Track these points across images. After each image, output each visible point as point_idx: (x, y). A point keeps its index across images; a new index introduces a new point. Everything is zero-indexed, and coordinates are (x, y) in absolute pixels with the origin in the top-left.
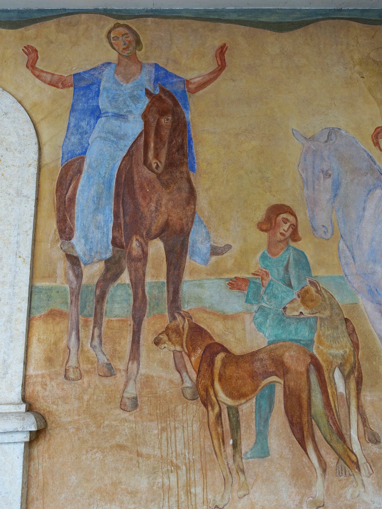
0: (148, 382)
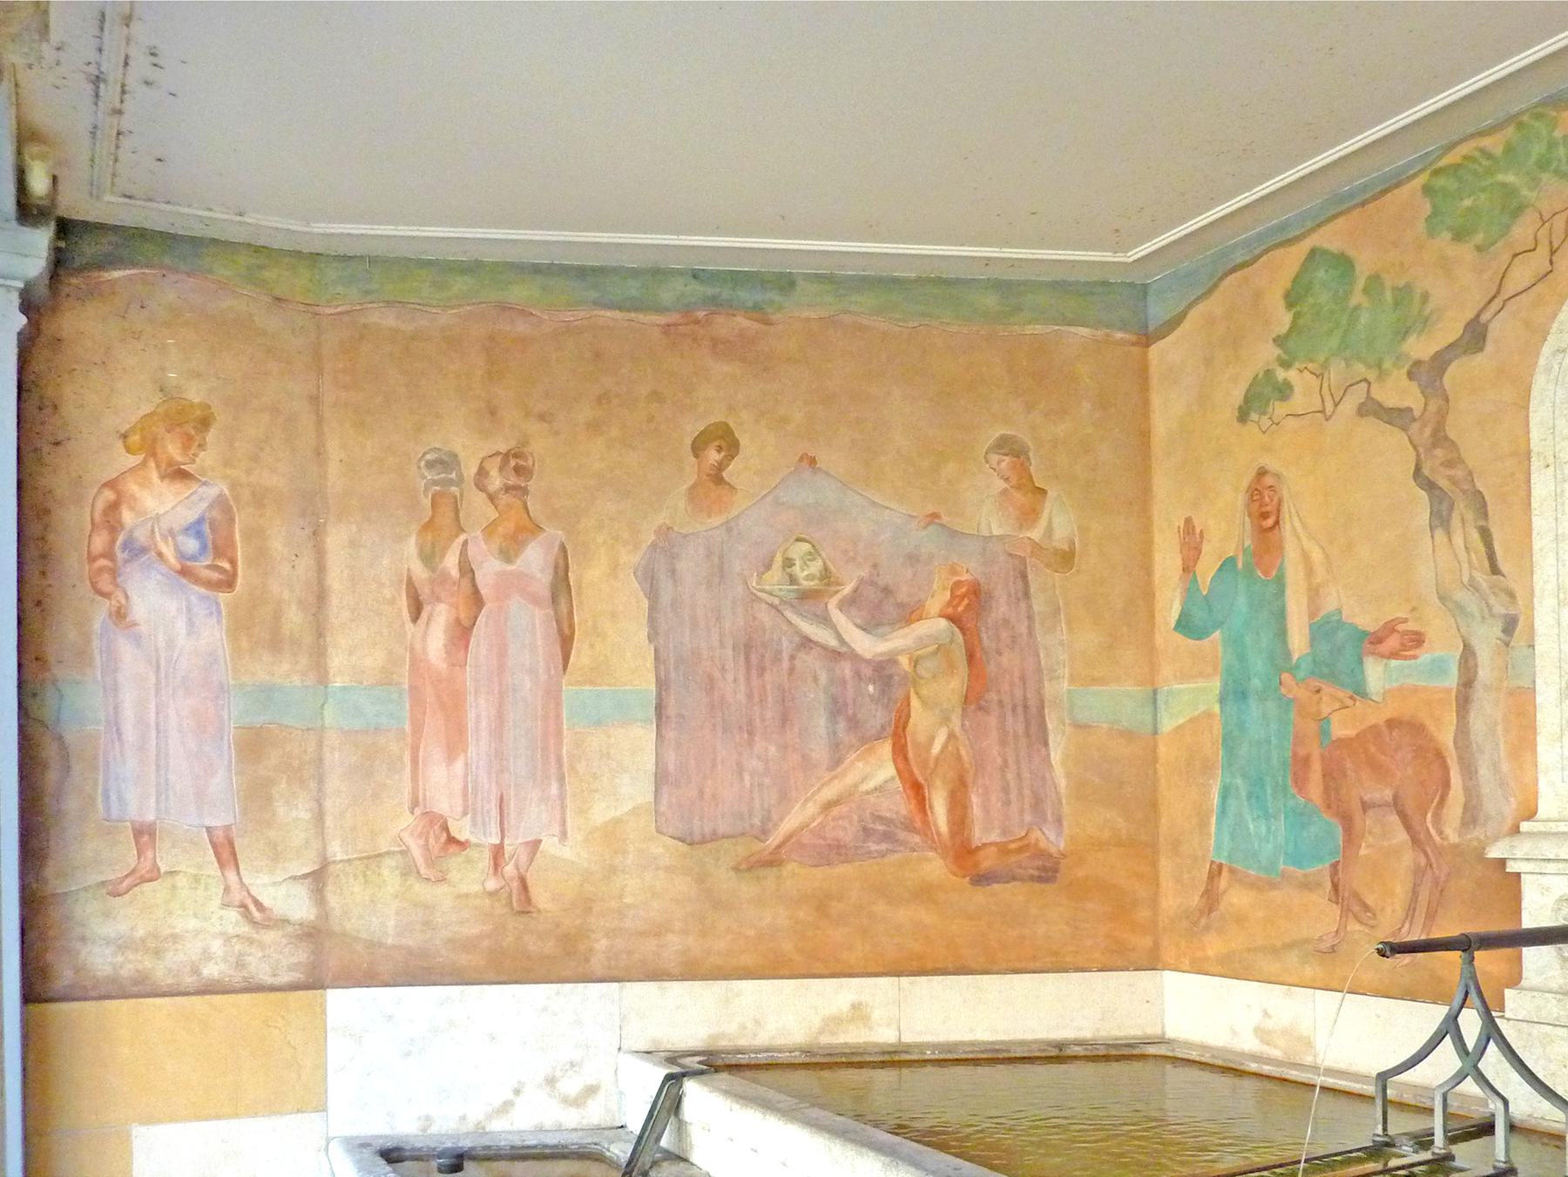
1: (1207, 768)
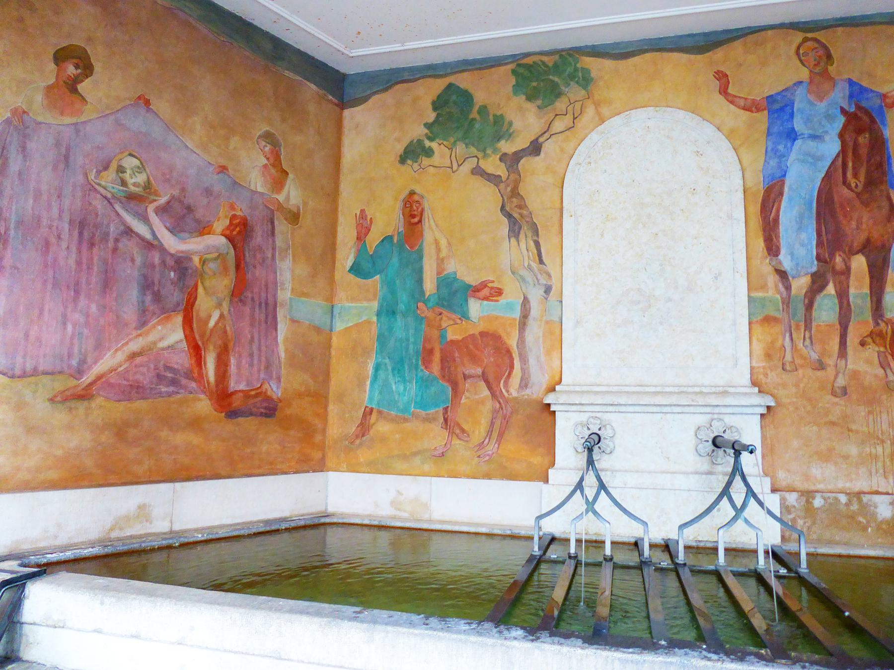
0: (855, 375)
1: (366, 352)
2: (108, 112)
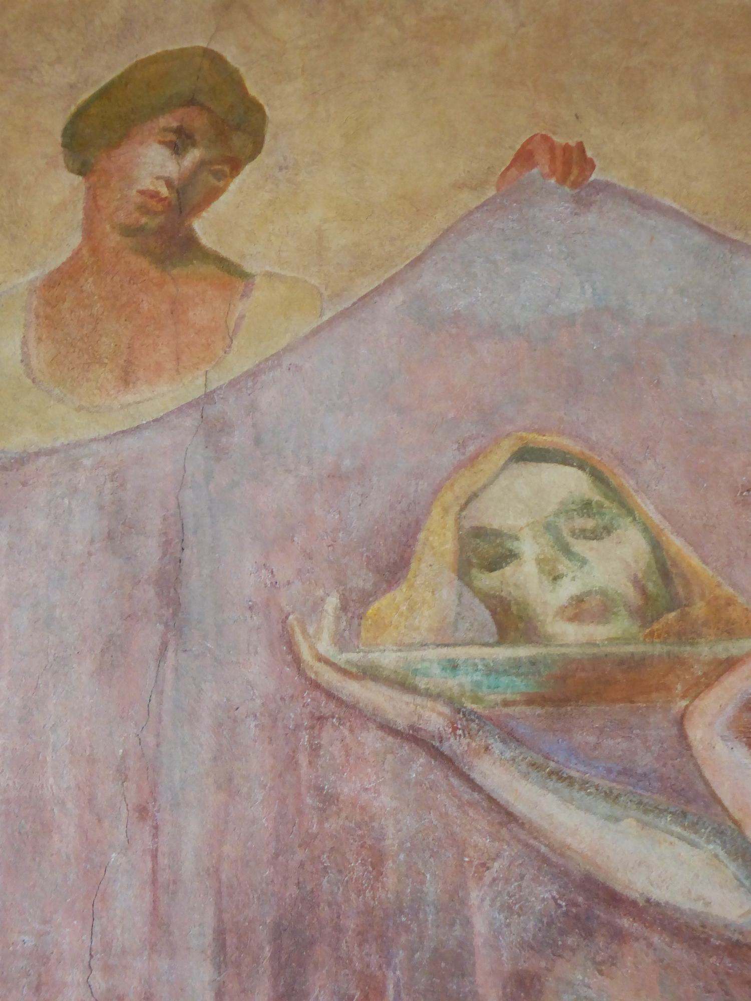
2: (363, 287)
